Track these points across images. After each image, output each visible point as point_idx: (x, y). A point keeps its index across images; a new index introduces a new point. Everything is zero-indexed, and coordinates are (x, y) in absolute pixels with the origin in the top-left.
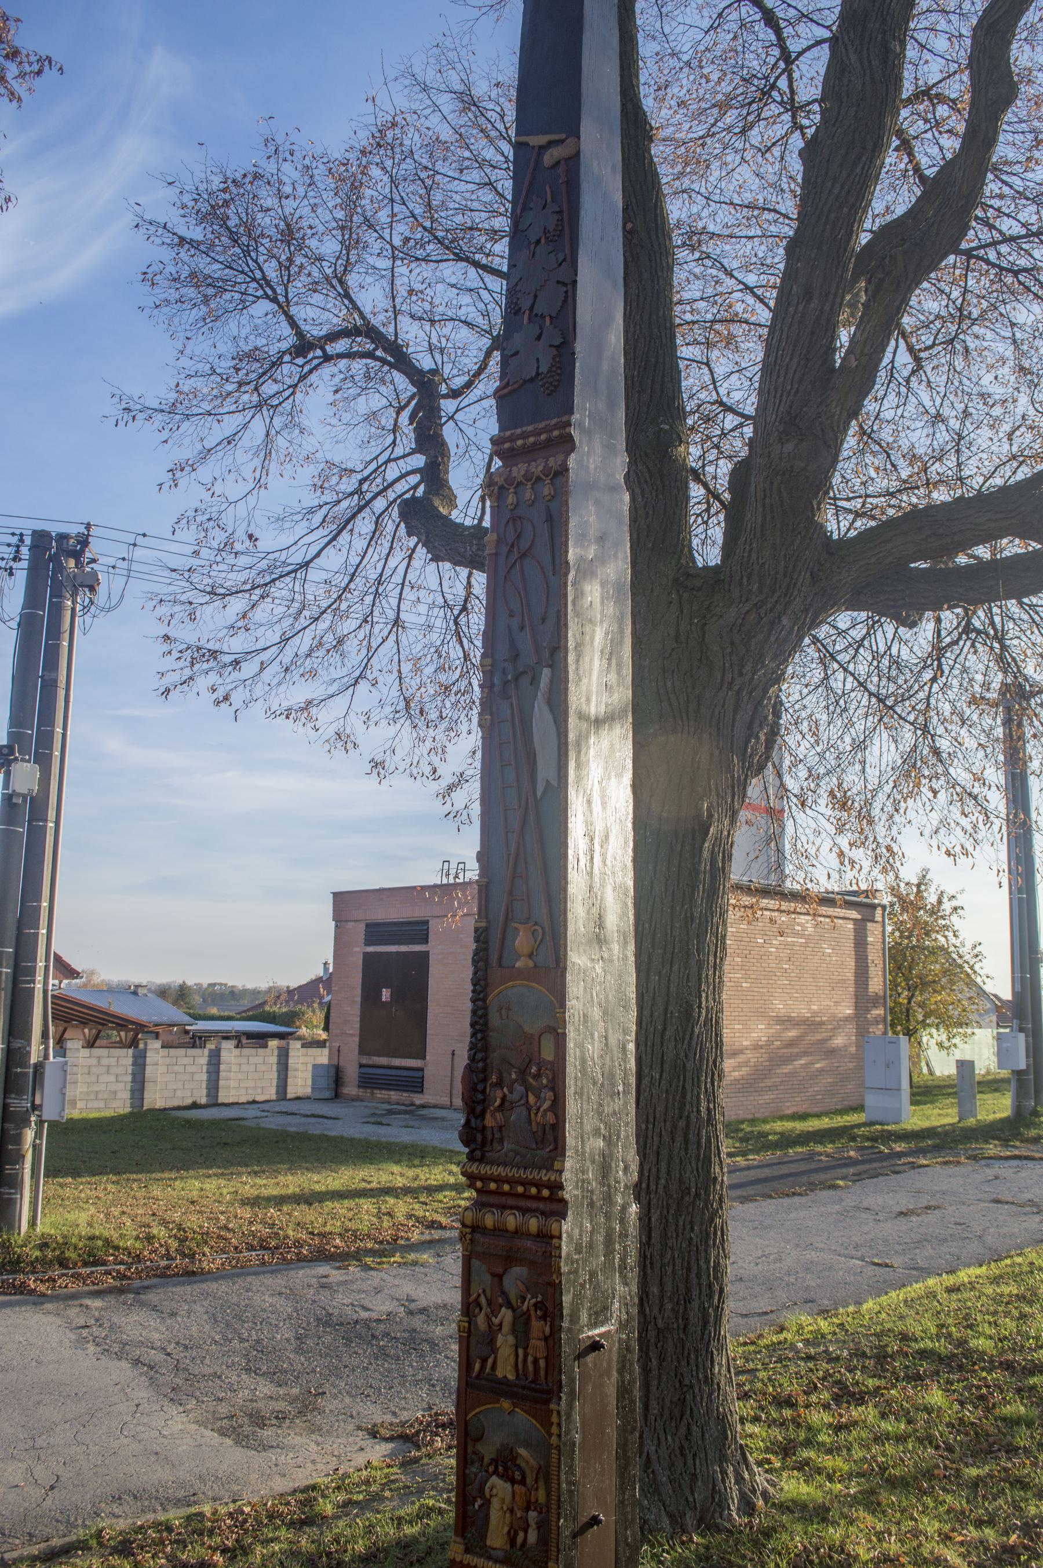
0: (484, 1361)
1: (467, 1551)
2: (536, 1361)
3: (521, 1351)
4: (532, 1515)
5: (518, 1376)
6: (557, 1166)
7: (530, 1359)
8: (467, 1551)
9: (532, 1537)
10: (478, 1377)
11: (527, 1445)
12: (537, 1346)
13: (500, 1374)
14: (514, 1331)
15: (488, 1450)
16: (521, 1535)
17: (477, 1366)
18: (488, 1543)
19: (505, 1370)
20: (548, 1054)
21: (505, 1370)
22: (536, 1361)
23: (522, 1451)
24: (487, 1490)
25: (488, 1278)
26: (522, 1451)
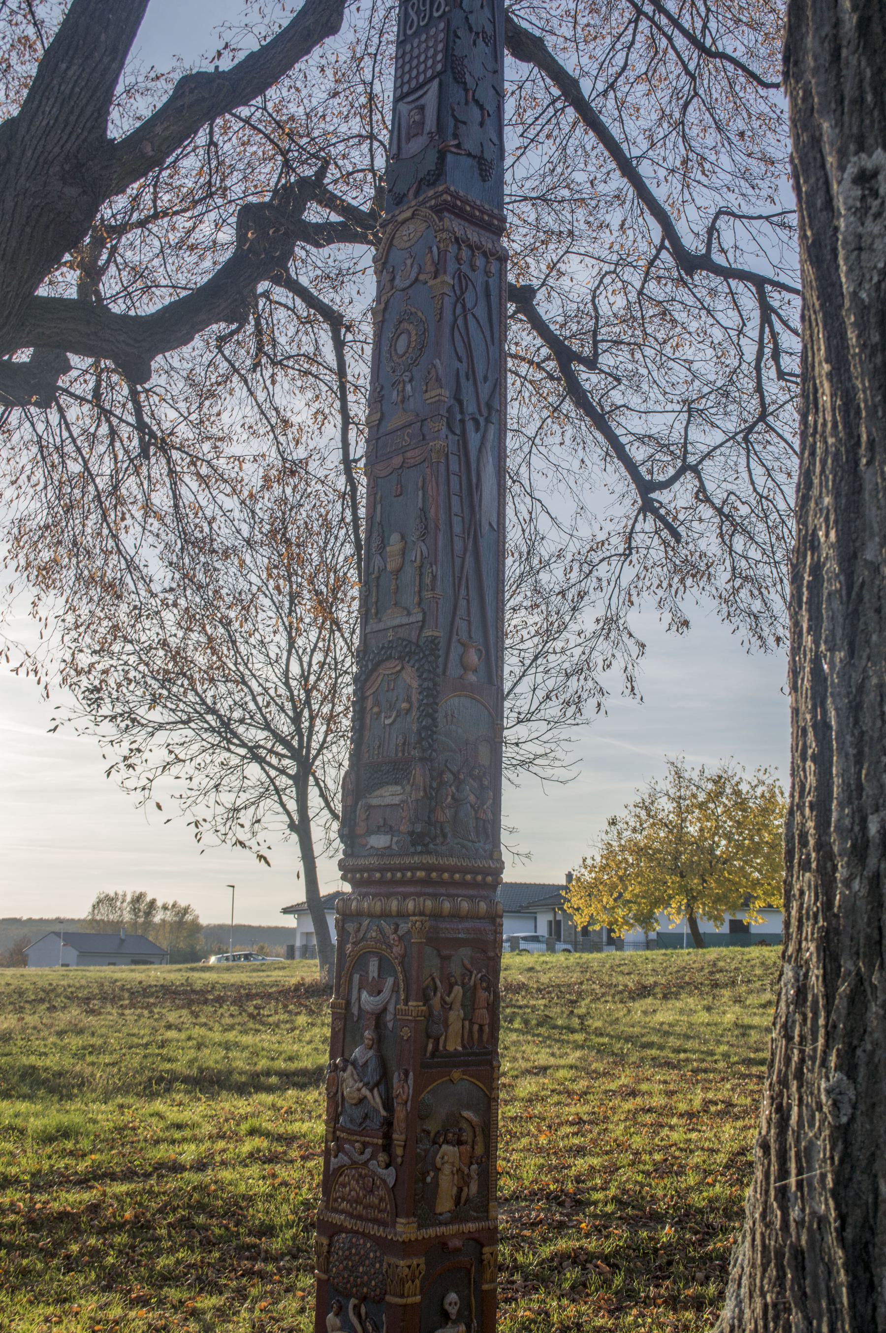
0: (437, 1040)
1: (420, 1227)
2: (481, 1027)
3: (467, 1023)
4: (474, 1167)
5: (464, 1047)
6: (495, 856)
7: (476, 1028)
8: (420, 1227)
9: (474, 1188)
10: (433, 1055)
11: (468, 1107)
12: (483, 1015)
13: (451, 1048)
14: (463, 1006)
15: (433, 1126)
16: (465, 1189)
17: (430, 1046)
18: (438, 1211)
19: (454, 1045)
20: (484, 758)
21: (454, 1045)
22: (481, 1027)
23: (467, 1114)
24: (438, 1159)
25: (437, 962)
26: (467, 1114)
